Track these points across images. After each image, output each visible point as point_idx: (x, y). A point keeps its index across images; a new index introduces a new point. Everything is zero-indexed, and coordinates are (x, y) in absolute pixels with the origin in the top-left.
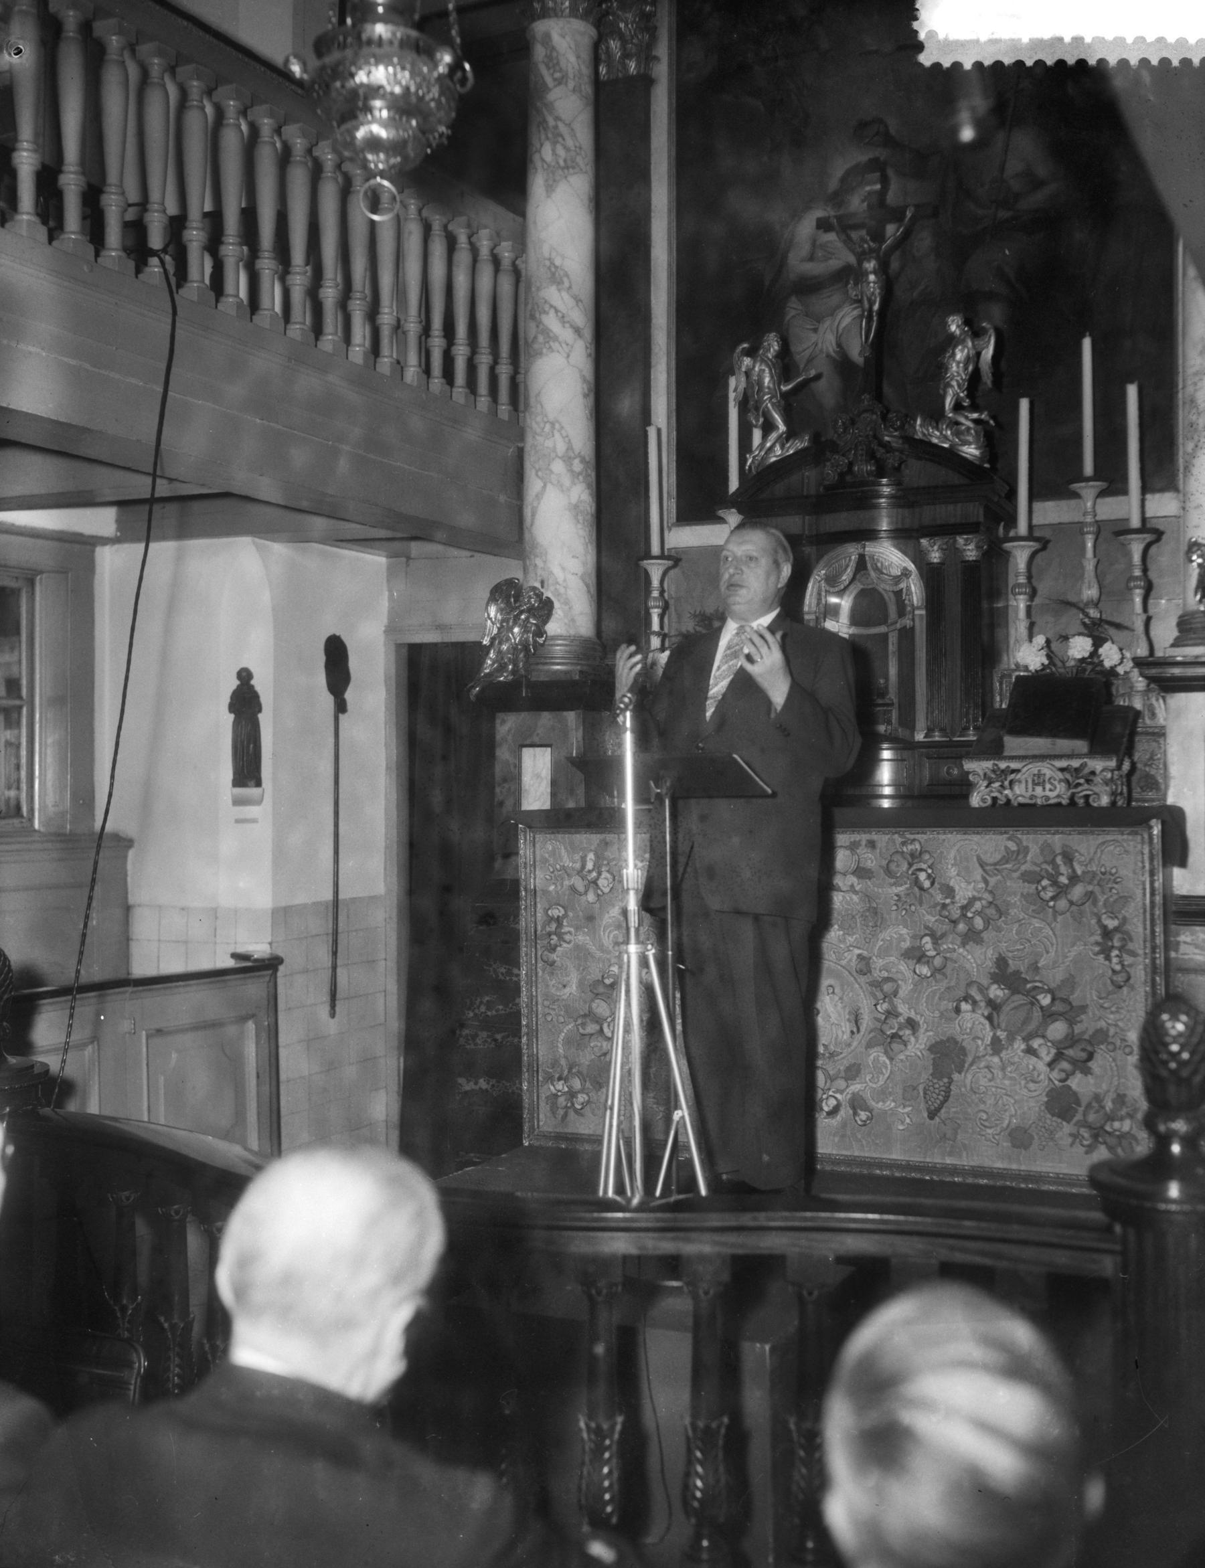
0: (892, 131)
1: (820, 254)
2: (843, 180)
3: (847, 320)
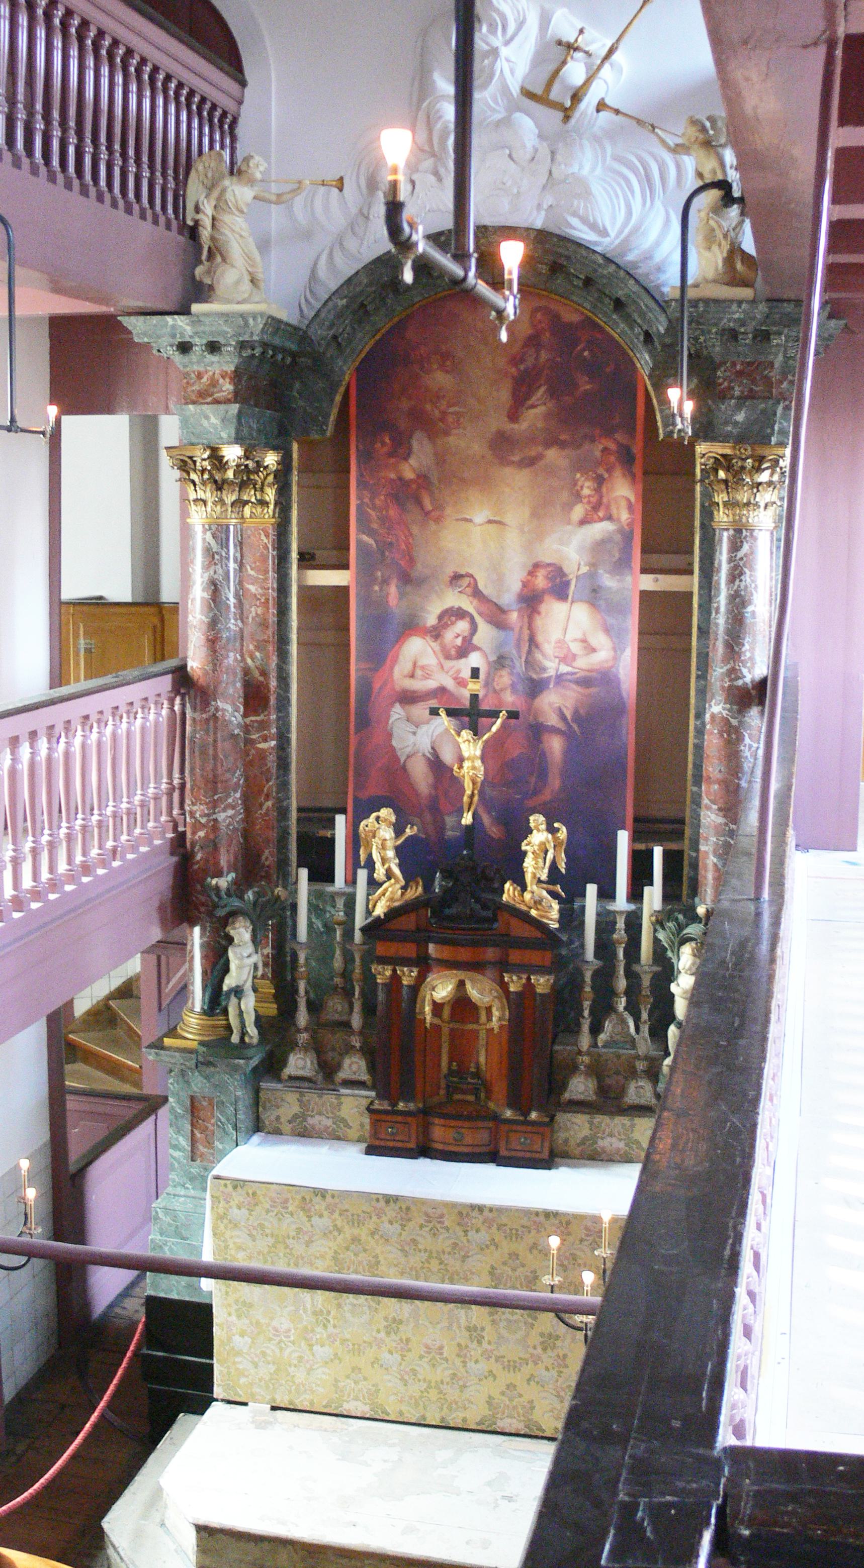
0: (481, 586)
2: (440, 617)
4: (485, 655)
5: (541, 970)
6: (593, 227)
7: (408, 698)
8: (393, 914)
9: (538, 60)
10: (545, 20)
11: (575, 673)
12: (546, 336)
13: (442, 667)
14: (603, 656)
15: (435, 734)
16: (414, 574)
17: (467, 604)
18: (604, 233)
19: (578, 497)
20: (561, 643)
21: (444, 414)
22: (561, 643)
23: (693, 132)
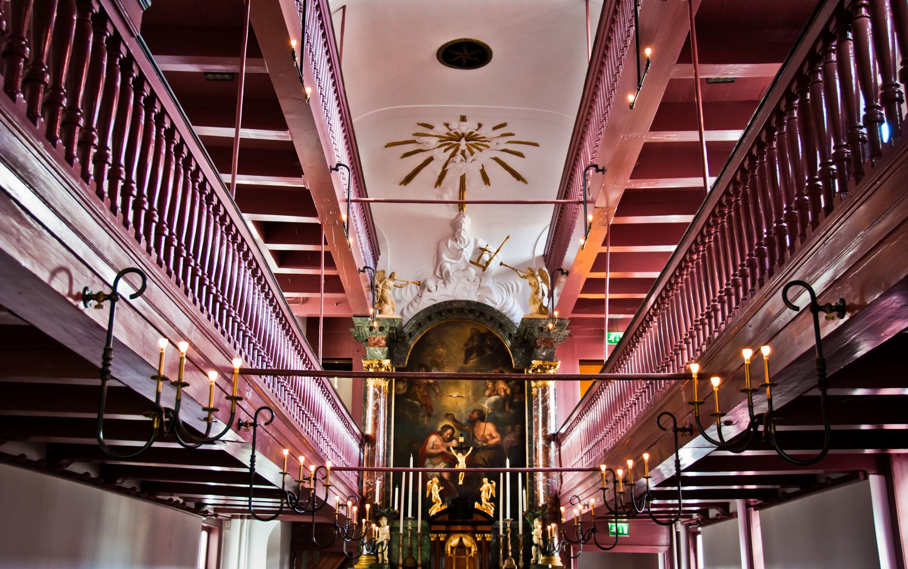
5: (488, 532)
6: (493, 302)
7: (432, 456)
8: (438, 514)
9: (474, 253)
10: (476, 242)
12: (476, 337)
14: (497, 439)
16: (434, 413)
17: (450, 423)
18: (496, 304)
19: (487, 388)
20: (483, 436)
21: (443, 362)
22: (483, 436)
23: (529, 271)
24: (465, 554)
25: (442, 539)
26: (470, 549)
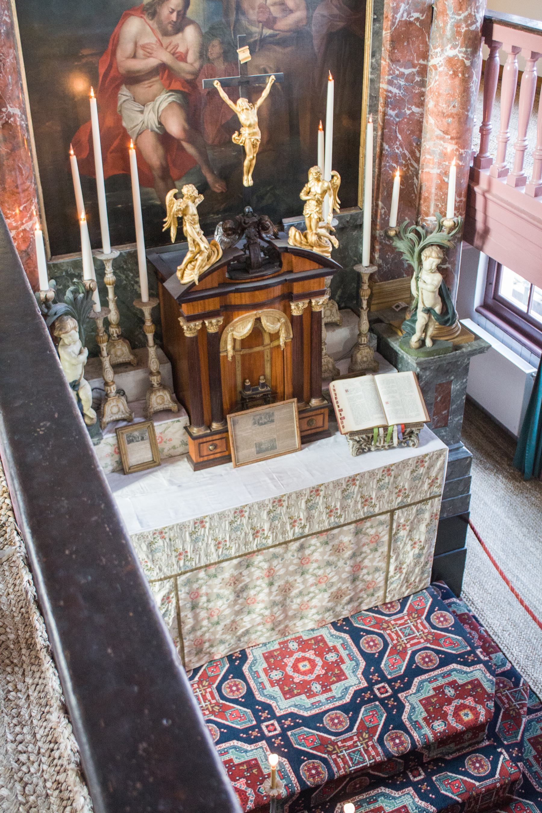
1: (140, 52)
3: (165, 105)
4: (198, 27)
7: (133, 79)
11: (276, 35)
13: (162, 45)
15: (161, 110)
24: (262, 344)
25: (212, 330)
26: (275, 336)
